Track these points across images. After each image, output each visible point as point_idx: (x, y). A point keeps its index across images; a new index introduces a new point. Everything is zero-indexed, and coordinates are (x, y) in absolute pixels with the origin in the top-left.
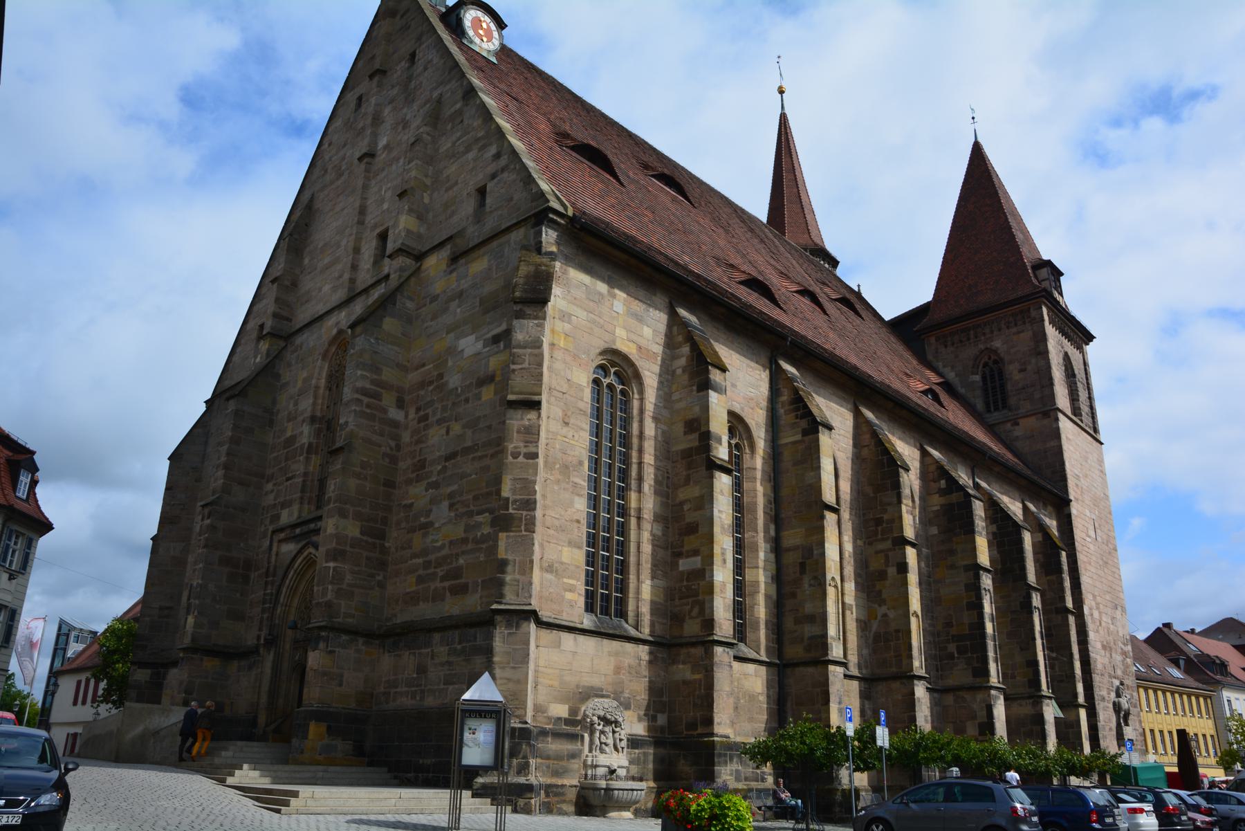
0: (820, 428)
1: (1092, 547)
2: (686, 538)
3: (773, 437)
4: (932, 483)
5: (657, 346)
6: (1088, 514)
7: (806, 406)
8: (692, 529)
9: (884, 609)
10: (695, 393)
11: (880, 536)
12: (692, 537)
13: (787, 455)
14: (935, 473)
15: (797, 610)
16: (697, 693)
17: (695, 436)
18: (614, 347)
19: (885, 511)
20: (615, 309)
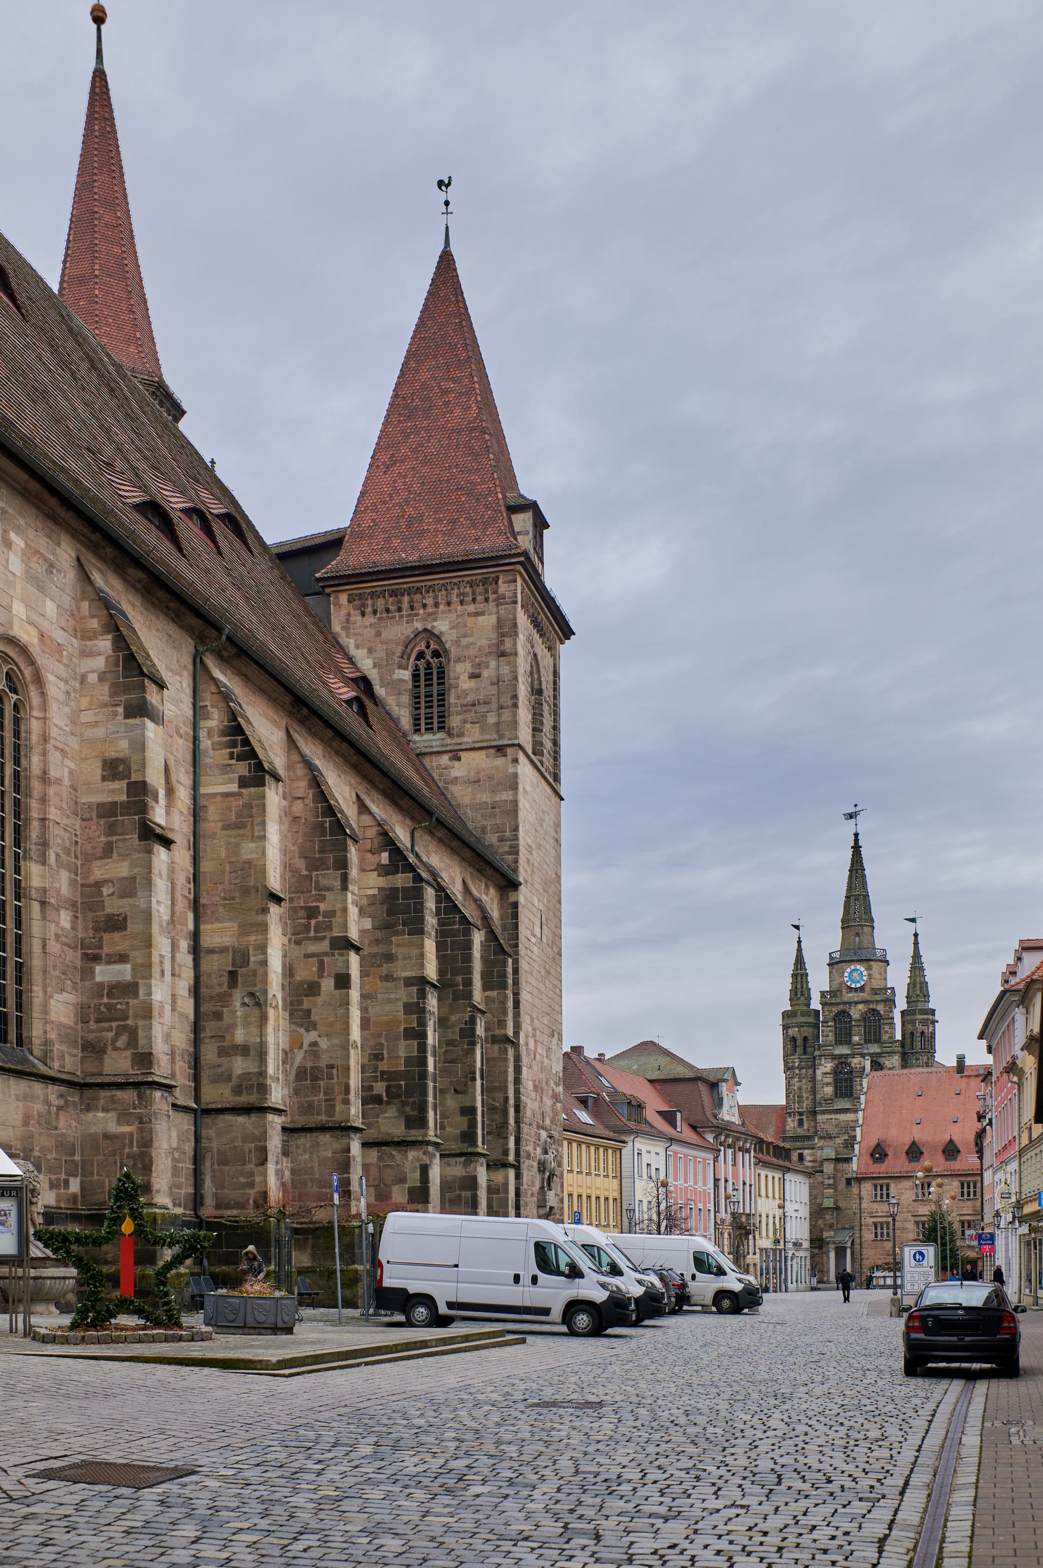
0: (267, 777)
1: (535, 949)
2: (106, 937)
3: (194, 782)
4: (369, 855)
5: (62, 632)
6: (536, 902)
7: (247, 742)
8: (116, 924)
9: (313, 1036)
10: (120, 718)
11: (312, 934)
12: (116, 935)
13: (213, 813)
14: (376, 841)
15: (223, 1037)
16: (126, 1151)
17: (122, 785)
18: (11, 633)
19: (323, 898)
20: (11, 568)
